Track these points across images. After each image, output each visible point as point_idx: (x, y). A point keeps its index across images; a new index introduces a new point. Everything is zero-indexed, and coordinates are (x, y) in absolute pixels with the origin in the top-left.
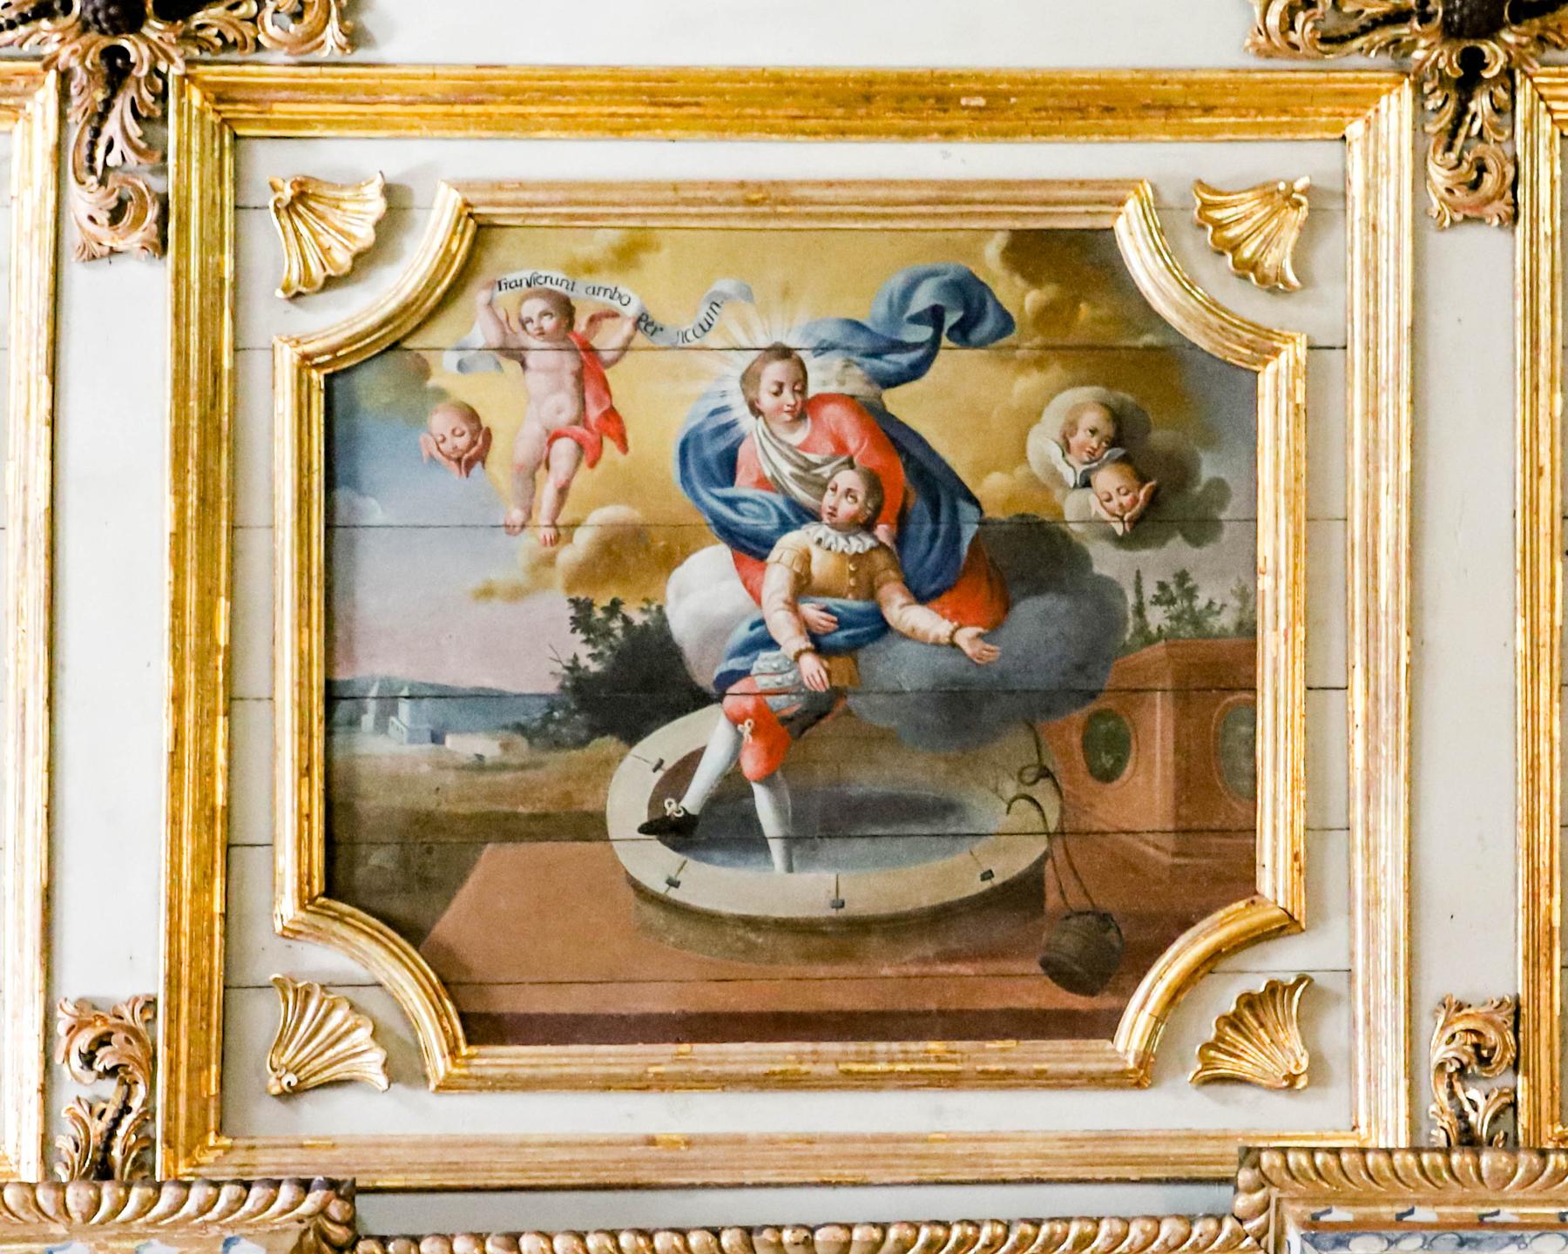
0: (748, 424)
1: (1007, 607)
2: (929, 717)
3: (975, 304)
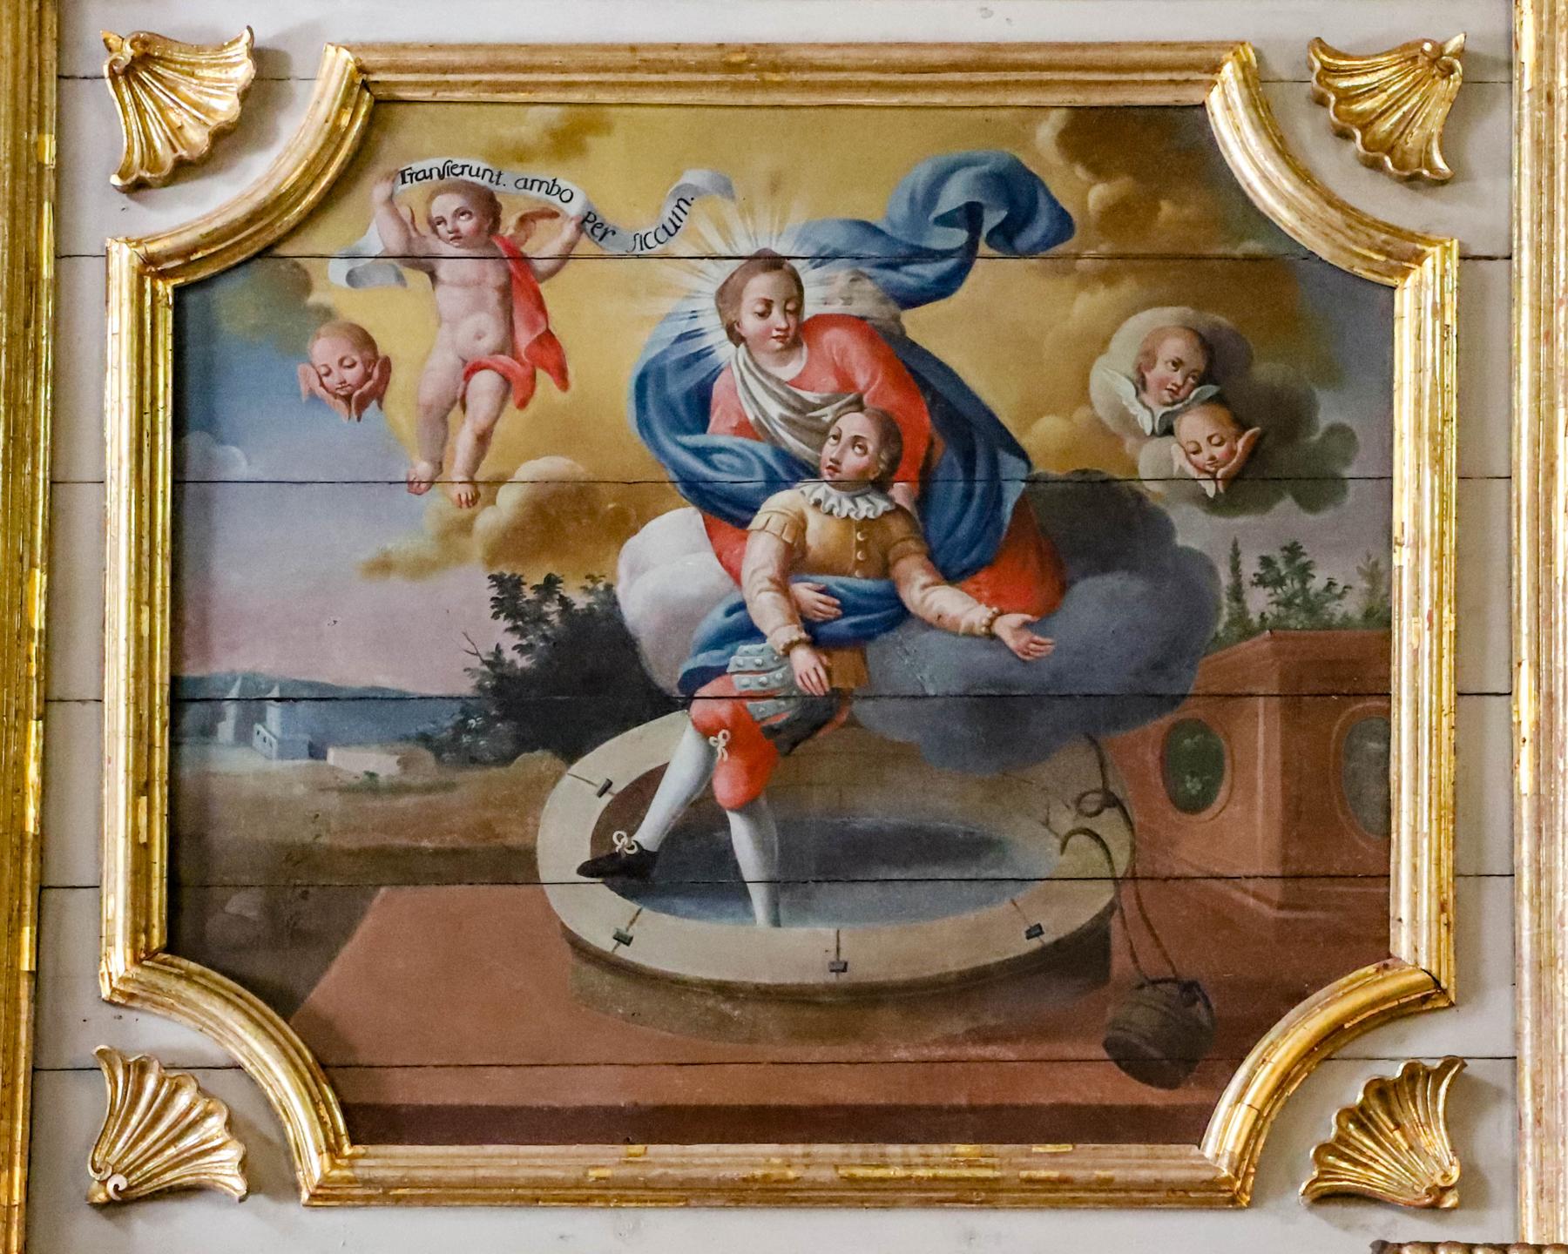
1: (1064, 588)
2: (959, 729)
3: (1023, 200)
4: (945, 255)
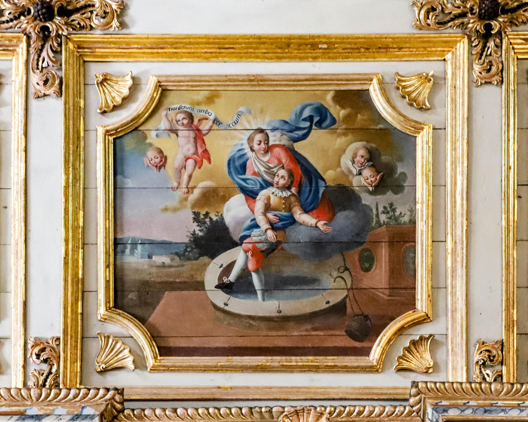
0: (250, 154)
1: (334, 215)
2: (309, 251)
3: (324, 114)
4: (304, 129)
